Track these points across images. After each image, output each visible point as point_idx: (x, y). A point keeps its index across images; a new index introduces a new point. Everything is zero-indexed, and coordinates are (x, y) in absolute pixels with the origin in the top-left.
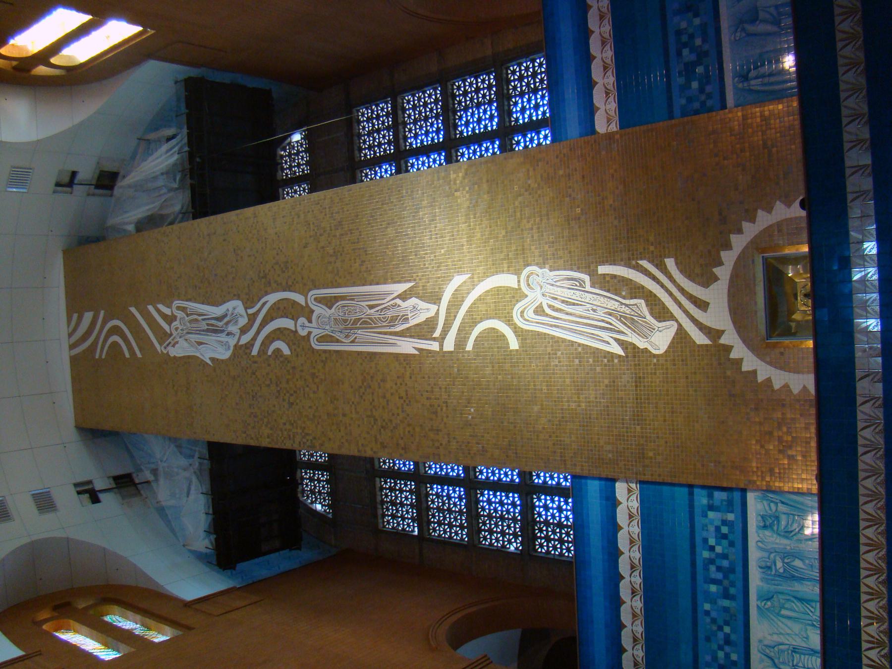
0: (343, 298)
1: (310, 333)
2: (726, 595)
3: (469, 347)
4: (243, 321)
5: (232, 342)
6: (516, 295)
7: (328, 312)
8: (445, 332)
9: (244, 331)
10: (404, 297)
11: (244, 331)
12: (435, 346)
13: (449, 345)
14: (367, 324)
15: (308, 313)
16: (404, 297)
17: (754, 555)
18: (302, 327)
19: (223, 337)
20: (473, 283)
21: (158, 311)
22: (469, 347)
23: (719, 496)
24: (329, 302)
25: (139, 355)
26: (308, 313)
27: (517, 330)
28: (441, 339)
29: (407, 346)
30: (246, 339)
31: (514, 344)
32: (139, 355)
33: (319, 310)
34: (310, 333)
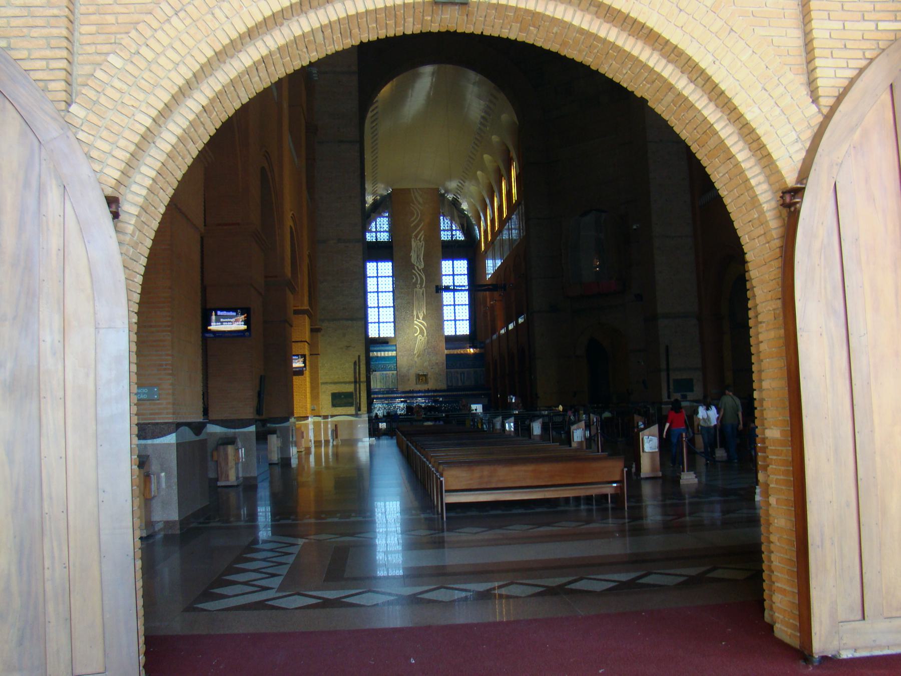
0: (423, 297)
1: (416, 288)
2: (382, 368)
3: (415, 326)
4: (420, 268)
5: (415, 263)
6: (423, 336)
7: (421, 293)
8: (417, 321)
9: (418, 268)
10: (423, 312)
11: (418, 268)
12: (415, 319)
13: (415, 322)
14: (419, 304)
15: (421, 288)
16: (423, 312)
17: (388, 372)
18: (418, 286)
19: (416, 260)
20: (425, 327)
21: (422, 235)
22: (415, 326)
23: (396, 367)
24: (423, 294)
25: (412, 225)
26: (421, 288)
27: (417, 336)
28: (416, 320)
29: (415, 313)
30: (416, 267)
31: (416, 335)
32: (412, 225)
33: (421, 291)
34: (416, 288)
